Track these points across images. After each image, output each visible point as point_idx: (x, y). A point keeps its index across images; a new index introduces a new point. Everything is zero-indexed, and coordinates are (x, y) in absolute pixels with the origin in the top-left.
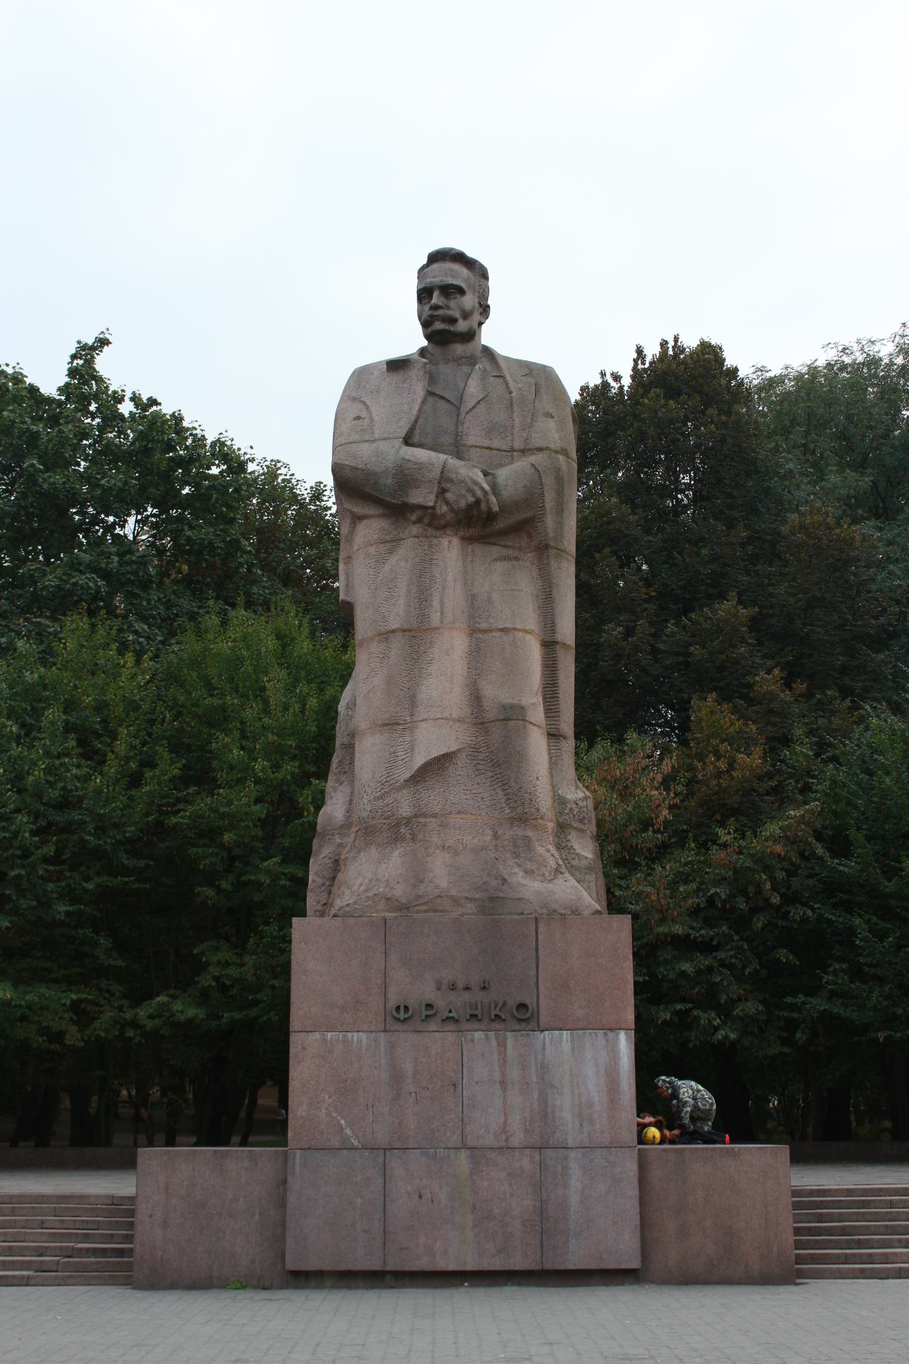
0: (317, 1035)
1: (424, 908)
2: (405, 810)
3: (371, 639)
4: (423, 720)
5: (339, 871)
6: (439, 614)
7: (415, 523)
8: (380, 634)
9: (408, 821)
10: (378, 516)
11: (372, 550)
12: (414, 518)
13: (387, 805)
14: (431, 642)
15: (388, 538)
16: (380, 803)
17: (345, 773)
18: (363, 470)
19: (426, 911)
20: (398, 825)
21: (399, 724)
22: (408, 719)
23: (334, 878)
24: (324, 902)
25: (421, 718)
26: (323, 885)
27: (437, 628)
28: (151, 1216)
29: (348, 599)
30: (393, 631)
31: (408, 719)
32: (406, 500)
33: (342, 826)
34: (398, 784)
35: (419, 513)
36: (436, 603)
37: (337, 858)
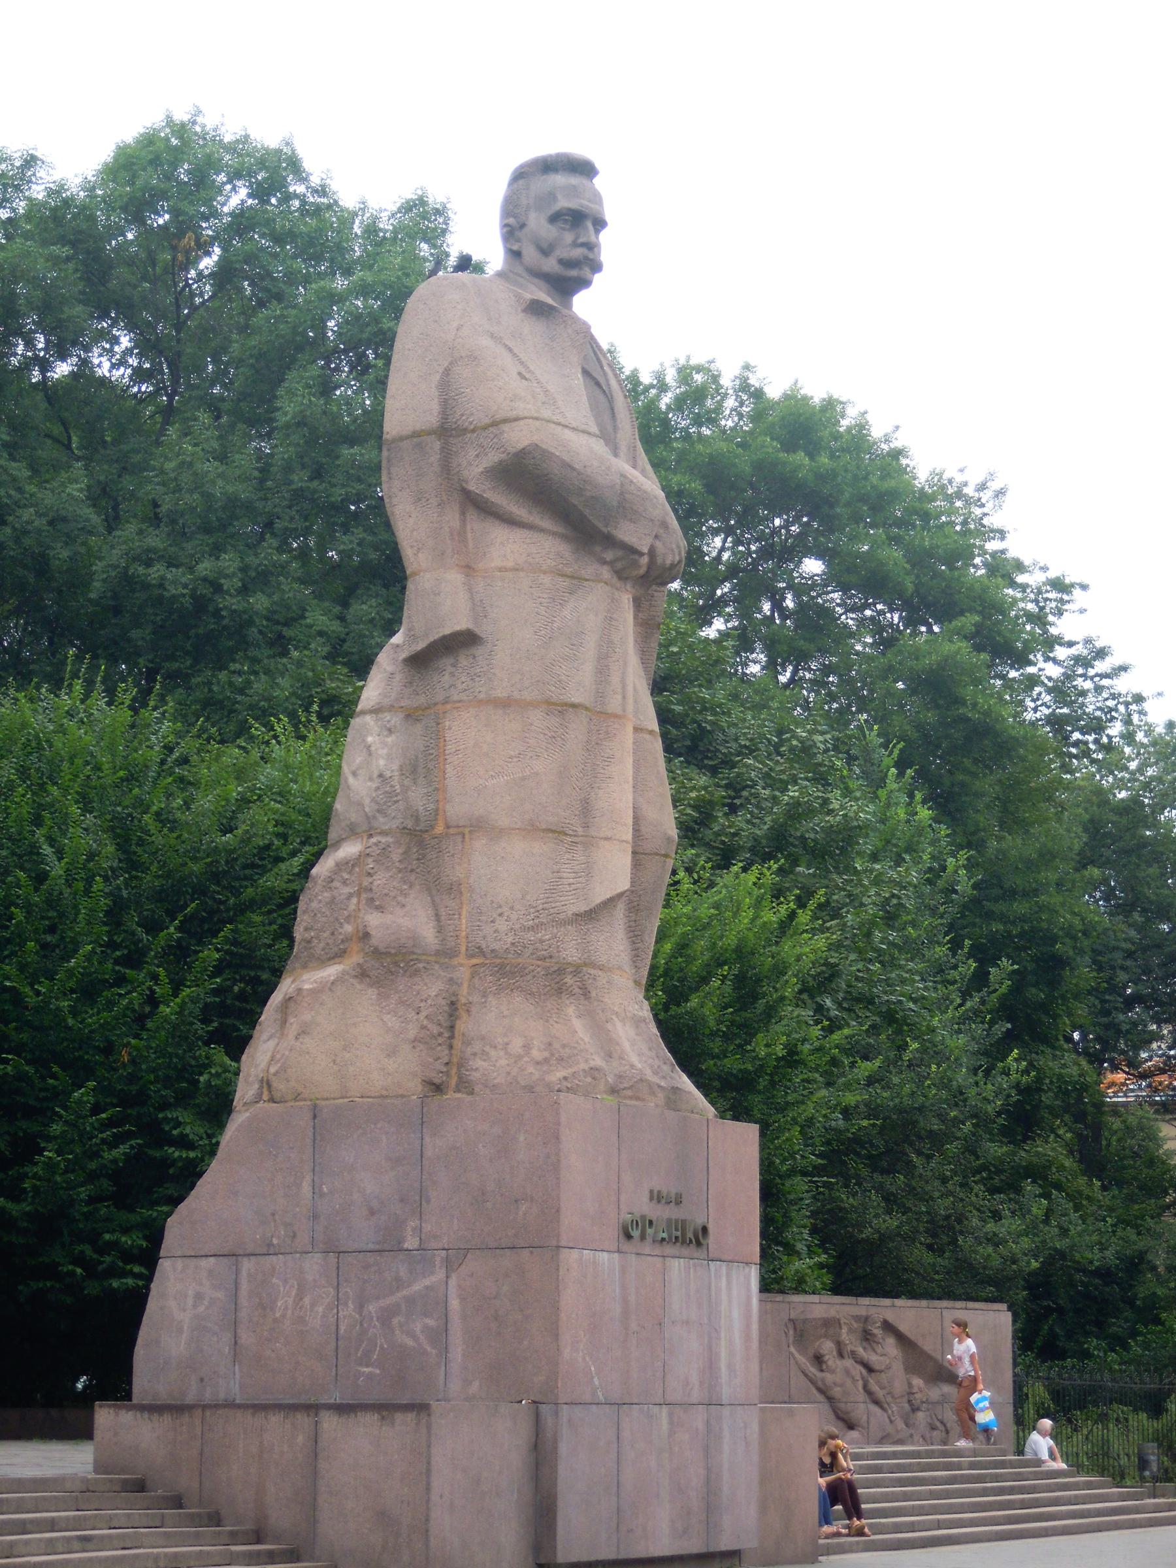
0: (575, 1254)
1: (629, 1093)
2: (571, 953)
3: (534, 704)
4: (607, 839)
5: (458, 1018)
6: (619, 697)
7: (604, 562)
8: (548, 703)
9: (577, 970)
10: (554, 534)
11: (546, 580)
12: (609, 555)
13: (541, 941)
14: (607, 733)
15: (569, 571)
16: (530, 936)
17: (412, 871)
18: (579, 473)
19: (631, 1098)
20: (561, 971)
21: (566, 834)
22: (580, 830)
23: (452, 1027)
24: (446, 1060)
25: (602, 835)
26: (440, 1034)
27: (616, 716)
28: (441, 1497)
29: (477, 631)
30: (574, 706)
31: (580, 830)
32: (614, 532)
33: (438, 953)
34: (562, 916)
35: (620, 553)
36: (615, 679)
37: (454, 999)
